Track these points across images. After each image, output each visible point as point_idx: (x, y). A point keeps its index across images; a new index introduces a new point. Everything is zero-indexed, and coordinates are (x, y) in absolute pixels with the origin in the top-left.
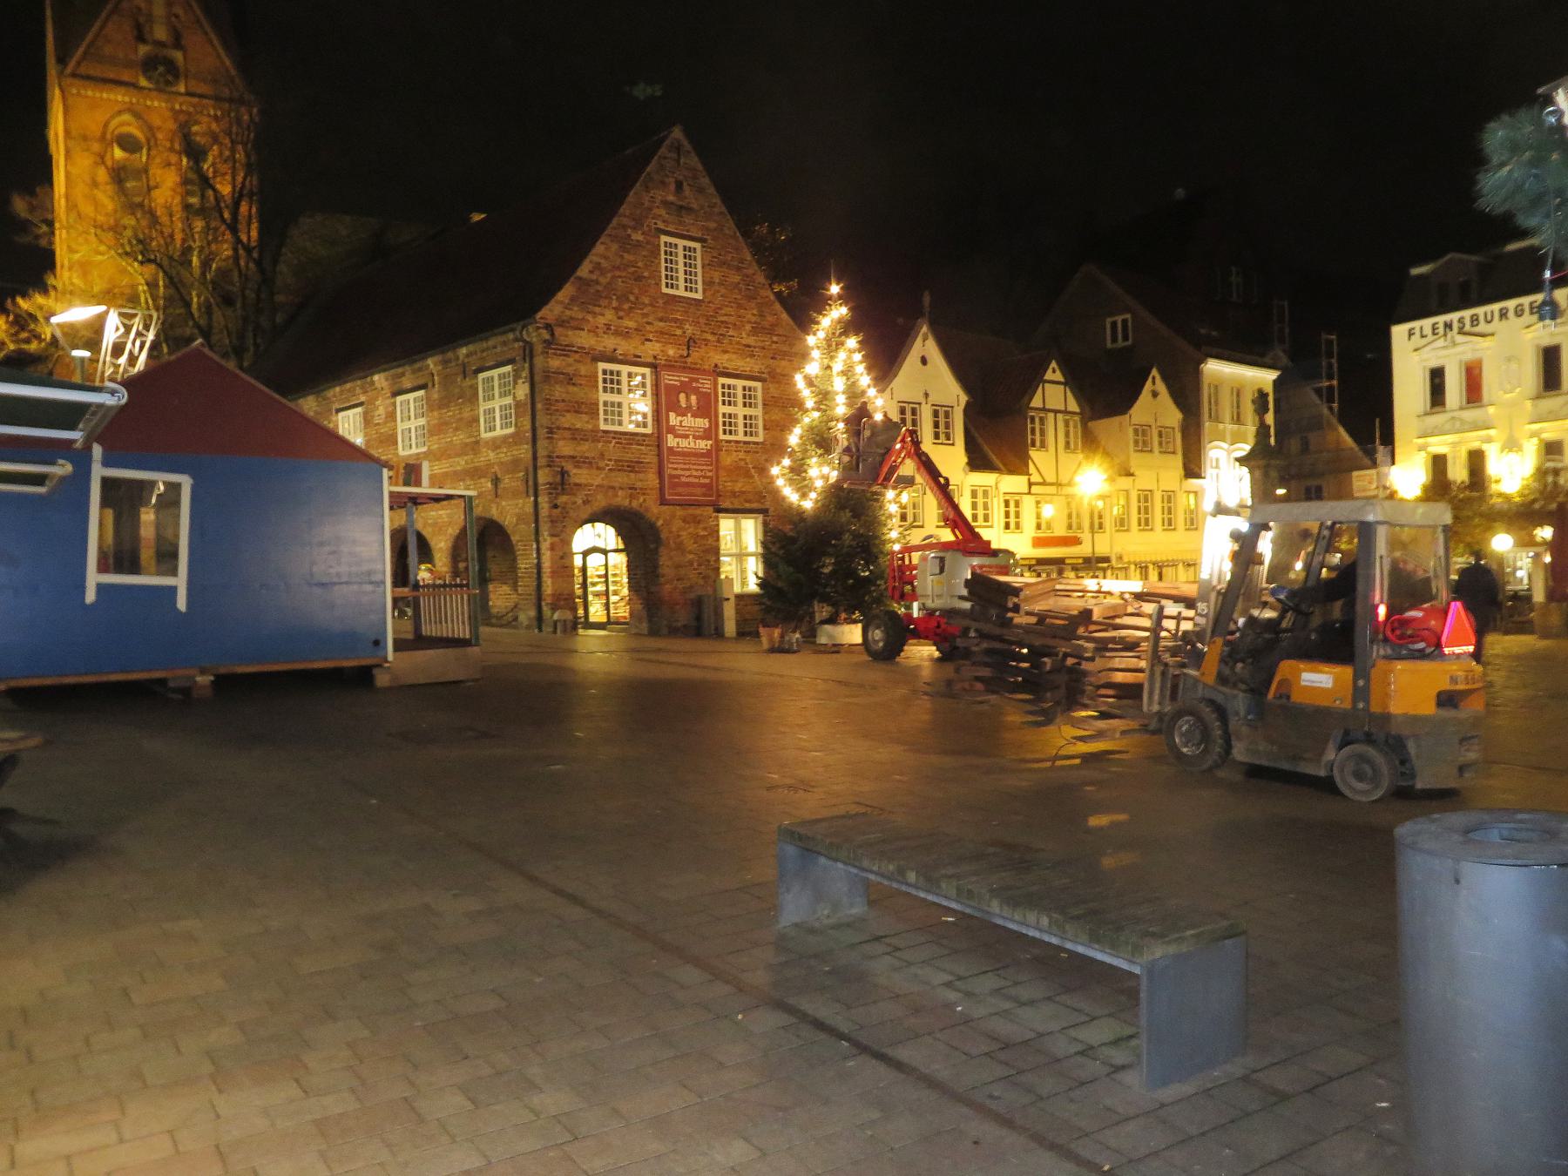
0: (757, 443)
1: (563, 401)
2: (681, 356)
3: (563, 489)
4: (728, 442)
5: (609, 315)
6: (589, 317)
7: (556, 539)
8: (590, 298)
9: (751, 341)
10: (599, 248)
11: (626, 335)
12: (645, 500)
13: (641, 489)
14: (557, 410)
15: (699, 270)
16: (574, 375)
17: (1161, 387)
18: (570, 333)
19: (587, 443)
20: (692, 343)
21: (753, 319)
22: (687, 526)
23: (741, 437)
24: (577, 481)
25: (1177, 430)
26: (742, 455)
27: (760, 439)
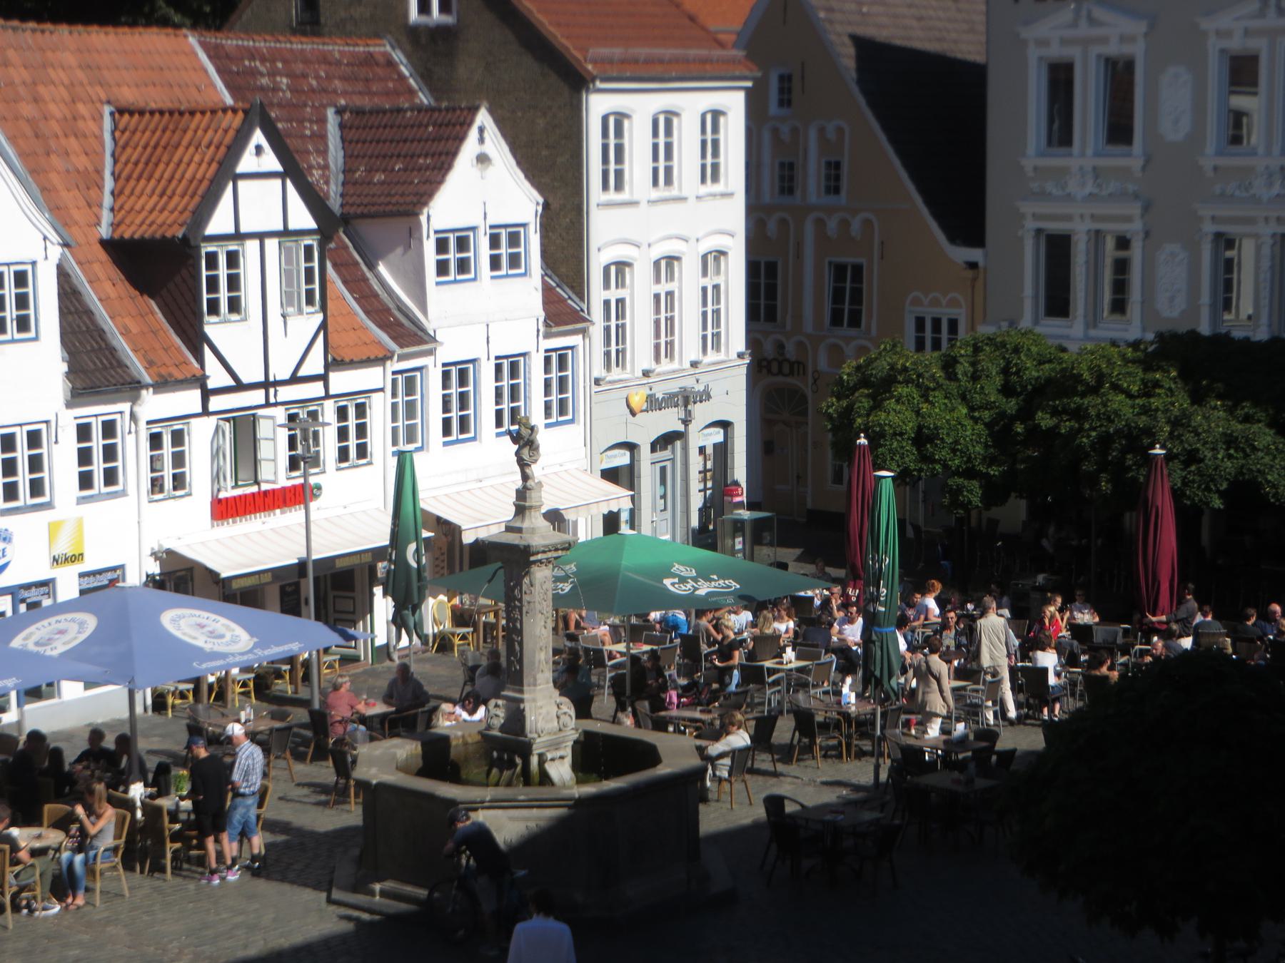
17: (496, 146)
25: (532, 228)
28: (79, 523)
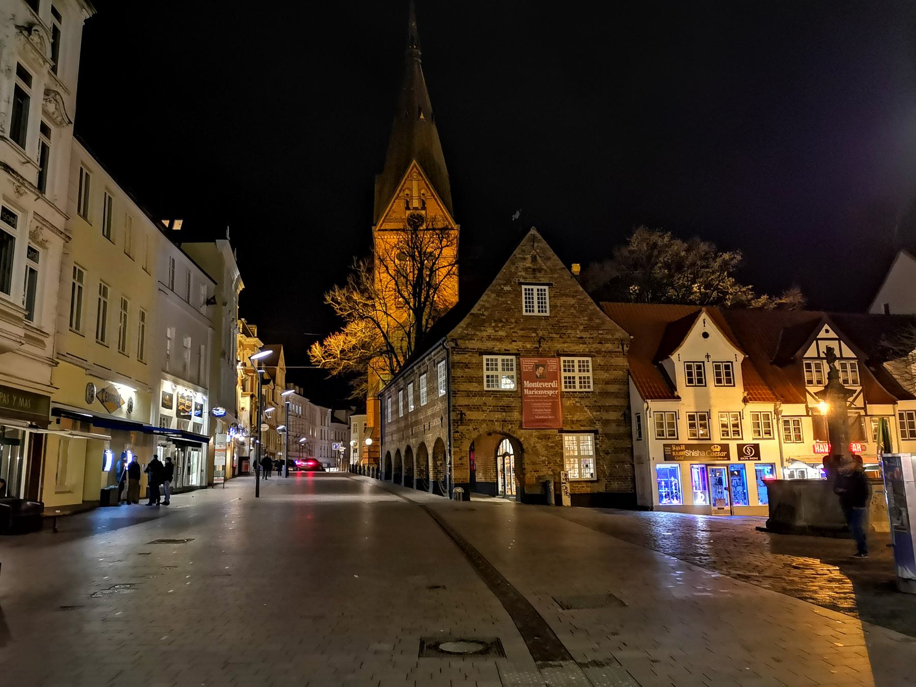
0: (589, 392)
1: (462, 377)
2: (537, 348)
3: (461, 423)
4: (566, 392)
5: (490, 331)
6: (478, 333)
7: (458, 449)
9: (585, 335)
10: (484, 297)
11: (500, 340)
13: (509, 421)
14: (459, 382)
15: (547, 301)
16: (468, 363)
18: (467, 342)
19: (476, 398)
20: (542, 340)
24: (469, 418)
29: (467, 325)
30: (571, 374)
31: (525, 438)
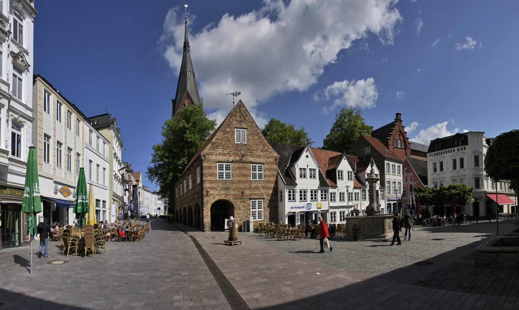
0: (262, 181)
1: (208, 174)
4: (253, 181)
6: (215, 152)
8: (215, 147)
9: (261, 154)
12: (229, 197)
13: (228, 194)
14: (206, 176)
18: (210, 156)
19: (214, 184)
21: (261, 148)
22: (241, 203)
23: (257, 179)
24: (211, 193)
26: (257, 184)
27: (263, 179)
28: (321, 203)
29: (210, 148)
30: (255, 172)
31: (235, 202)
